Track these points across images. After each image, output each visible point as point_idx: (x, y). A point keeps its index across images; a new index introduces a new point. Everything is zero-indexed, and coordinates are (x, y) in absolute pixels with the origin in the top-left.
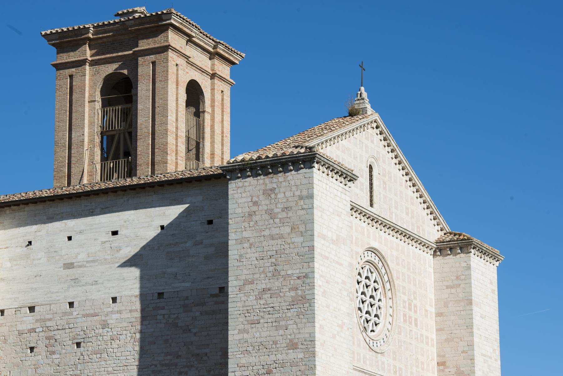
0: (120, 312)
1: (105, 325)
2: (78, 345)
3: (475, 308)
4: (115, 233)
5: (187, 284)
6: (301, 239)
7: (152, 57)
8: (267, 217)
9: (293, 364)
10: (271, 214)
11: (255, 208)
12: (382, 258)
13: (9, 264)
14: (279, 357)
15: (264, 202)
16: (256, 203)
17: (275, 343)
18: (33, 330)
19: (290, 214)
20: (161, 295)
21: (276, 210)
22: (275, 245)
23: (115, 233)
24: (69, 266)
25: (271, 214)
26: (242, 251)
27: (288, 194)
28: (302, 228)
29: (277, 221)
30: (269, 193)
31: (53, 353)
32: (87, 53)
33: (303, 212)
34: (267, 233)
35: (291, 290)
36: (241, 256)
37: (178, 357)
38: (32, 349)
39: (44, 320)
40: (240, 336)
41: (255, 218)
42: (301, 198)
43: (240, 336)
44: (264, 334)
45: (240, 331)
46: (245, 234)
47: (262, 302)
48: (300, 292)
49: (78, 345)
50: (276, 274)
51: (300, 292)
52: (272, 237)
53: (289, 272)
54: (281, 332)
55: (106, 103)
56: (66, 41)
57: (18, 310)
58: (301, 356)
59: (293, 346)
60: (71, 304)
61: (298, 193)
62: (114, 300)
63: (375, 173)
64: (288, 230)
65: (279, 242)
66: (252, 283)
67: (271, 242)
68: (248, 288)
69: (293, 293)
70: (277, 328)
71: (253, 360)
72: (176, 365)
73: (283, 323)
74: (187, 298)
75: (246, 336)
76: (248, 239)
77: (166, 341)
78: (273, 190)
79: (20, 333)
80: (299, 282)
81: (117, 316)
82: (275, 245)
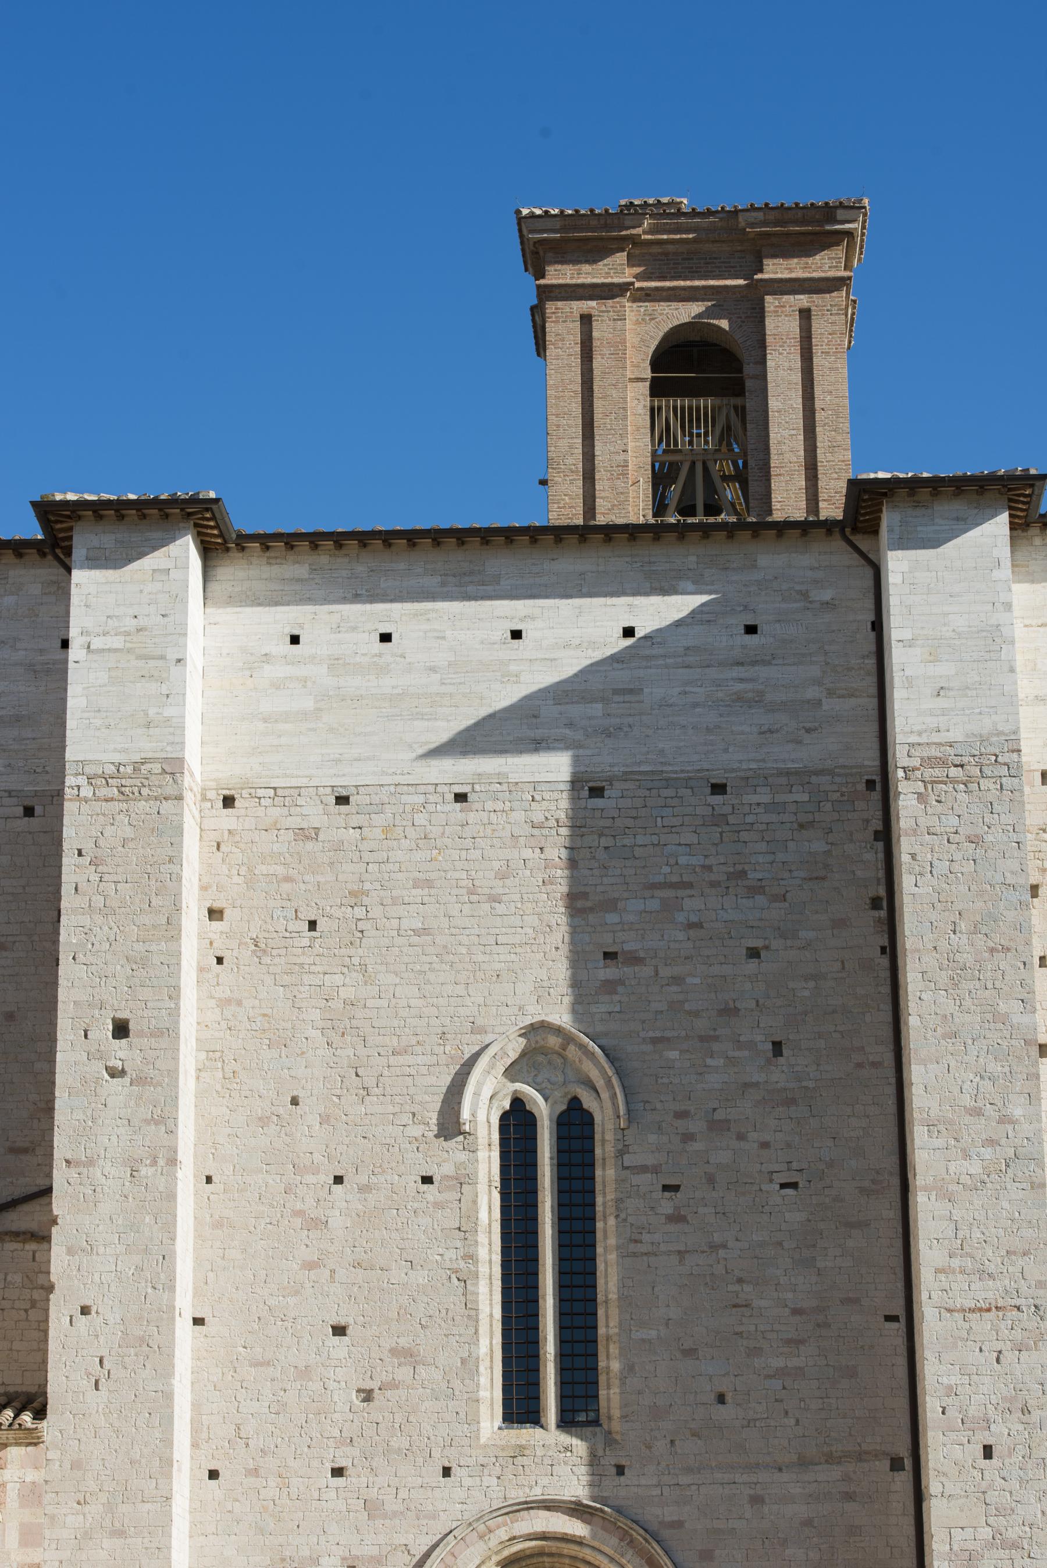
7: (803, 300)
32: (616, 269)
55: (657, 389)
56: (584, 236)
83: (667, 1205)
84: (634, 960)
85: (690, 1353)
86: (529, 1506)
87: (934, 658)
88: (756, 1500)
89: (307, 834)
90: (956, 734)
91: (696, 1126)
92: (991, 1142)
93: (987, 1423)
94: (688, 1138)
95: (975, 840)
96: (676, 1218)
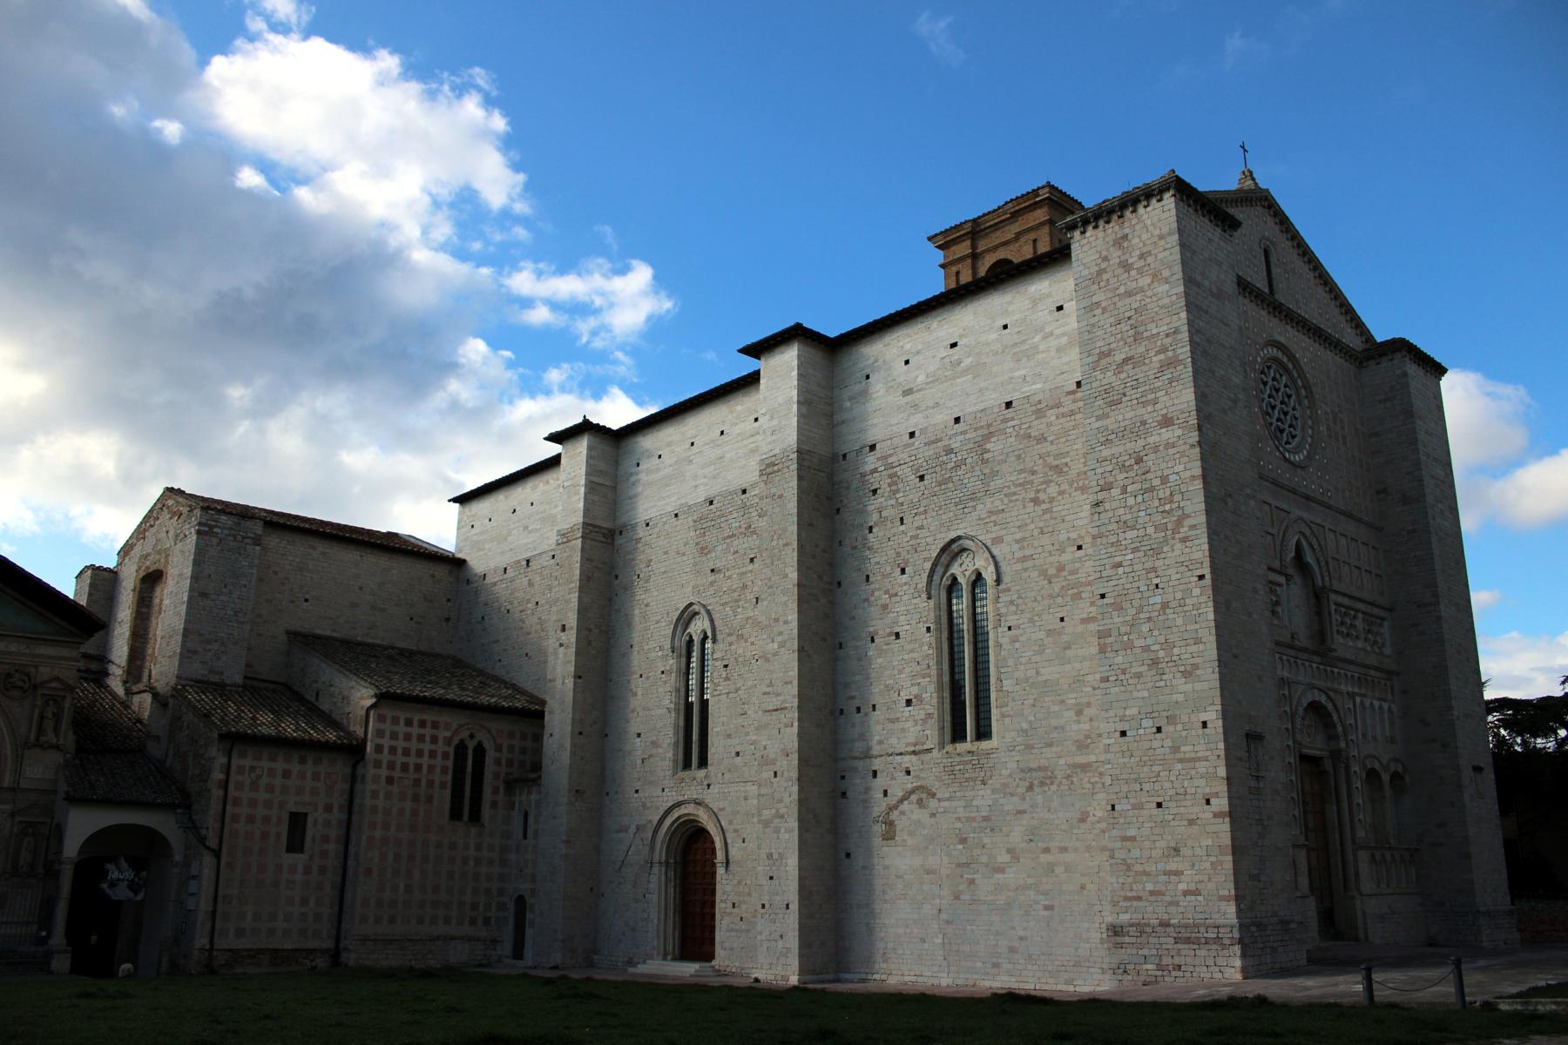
2: (922, 478)
3: (1419, 422)
4: (954, 345)
5: (1039, 386)
8: (1121, 270)
9: (1168, 445)
10: (1126, 267)
12: (1292, 358)
14: (1151, 440)
15: (1115, 255)
16: (1105, 259)
17: (1144, 423)
19: (1150, 260)
20: (1009, 405)
22: (1135, 302)
23: (954, 345)
25: (1126, 267)
26: (1092, 321)
27: (1144, 237)
29: (1133, 273)
31: (898, 491)
33: (1167, 253)
34: (1122, 290)
35: (1158, 353)
37: (1033, 473)
39: (886, 458)
40: (1099, 424)
41: (1105, 277)
42: (1161, 237)
43: (1099, 424)
44: (1128, 416)
45: (1099, 418)
46: (1095, 299)
47: (1123, 376)
48: (1170, 354)
50: (1137, 338)
51: (1170, 354)
52: (1129, 294)
54: (1150, 409)
58: (1179, 432)
59: (1167, 422)
61: (1157, 232)
63: (1273, 259)
65: (1139, 297)
66: (1109, 355)
67: (1128, 301)
68: (1103, 362)
69: (1162, 357)
71: (1116, 450)
72: (1032, 482)
77: (1019, 457)
78: (1125, 237)
80: (1169, 340)
81: (961, 438)
82: (1135, 302)
85: (729, 736)
86: (678, 805)
87: (772, 418)
90: (777, 451)
92: (781, 633)
93: (774, 762)
95: (781, 496)
96: (727, 679)
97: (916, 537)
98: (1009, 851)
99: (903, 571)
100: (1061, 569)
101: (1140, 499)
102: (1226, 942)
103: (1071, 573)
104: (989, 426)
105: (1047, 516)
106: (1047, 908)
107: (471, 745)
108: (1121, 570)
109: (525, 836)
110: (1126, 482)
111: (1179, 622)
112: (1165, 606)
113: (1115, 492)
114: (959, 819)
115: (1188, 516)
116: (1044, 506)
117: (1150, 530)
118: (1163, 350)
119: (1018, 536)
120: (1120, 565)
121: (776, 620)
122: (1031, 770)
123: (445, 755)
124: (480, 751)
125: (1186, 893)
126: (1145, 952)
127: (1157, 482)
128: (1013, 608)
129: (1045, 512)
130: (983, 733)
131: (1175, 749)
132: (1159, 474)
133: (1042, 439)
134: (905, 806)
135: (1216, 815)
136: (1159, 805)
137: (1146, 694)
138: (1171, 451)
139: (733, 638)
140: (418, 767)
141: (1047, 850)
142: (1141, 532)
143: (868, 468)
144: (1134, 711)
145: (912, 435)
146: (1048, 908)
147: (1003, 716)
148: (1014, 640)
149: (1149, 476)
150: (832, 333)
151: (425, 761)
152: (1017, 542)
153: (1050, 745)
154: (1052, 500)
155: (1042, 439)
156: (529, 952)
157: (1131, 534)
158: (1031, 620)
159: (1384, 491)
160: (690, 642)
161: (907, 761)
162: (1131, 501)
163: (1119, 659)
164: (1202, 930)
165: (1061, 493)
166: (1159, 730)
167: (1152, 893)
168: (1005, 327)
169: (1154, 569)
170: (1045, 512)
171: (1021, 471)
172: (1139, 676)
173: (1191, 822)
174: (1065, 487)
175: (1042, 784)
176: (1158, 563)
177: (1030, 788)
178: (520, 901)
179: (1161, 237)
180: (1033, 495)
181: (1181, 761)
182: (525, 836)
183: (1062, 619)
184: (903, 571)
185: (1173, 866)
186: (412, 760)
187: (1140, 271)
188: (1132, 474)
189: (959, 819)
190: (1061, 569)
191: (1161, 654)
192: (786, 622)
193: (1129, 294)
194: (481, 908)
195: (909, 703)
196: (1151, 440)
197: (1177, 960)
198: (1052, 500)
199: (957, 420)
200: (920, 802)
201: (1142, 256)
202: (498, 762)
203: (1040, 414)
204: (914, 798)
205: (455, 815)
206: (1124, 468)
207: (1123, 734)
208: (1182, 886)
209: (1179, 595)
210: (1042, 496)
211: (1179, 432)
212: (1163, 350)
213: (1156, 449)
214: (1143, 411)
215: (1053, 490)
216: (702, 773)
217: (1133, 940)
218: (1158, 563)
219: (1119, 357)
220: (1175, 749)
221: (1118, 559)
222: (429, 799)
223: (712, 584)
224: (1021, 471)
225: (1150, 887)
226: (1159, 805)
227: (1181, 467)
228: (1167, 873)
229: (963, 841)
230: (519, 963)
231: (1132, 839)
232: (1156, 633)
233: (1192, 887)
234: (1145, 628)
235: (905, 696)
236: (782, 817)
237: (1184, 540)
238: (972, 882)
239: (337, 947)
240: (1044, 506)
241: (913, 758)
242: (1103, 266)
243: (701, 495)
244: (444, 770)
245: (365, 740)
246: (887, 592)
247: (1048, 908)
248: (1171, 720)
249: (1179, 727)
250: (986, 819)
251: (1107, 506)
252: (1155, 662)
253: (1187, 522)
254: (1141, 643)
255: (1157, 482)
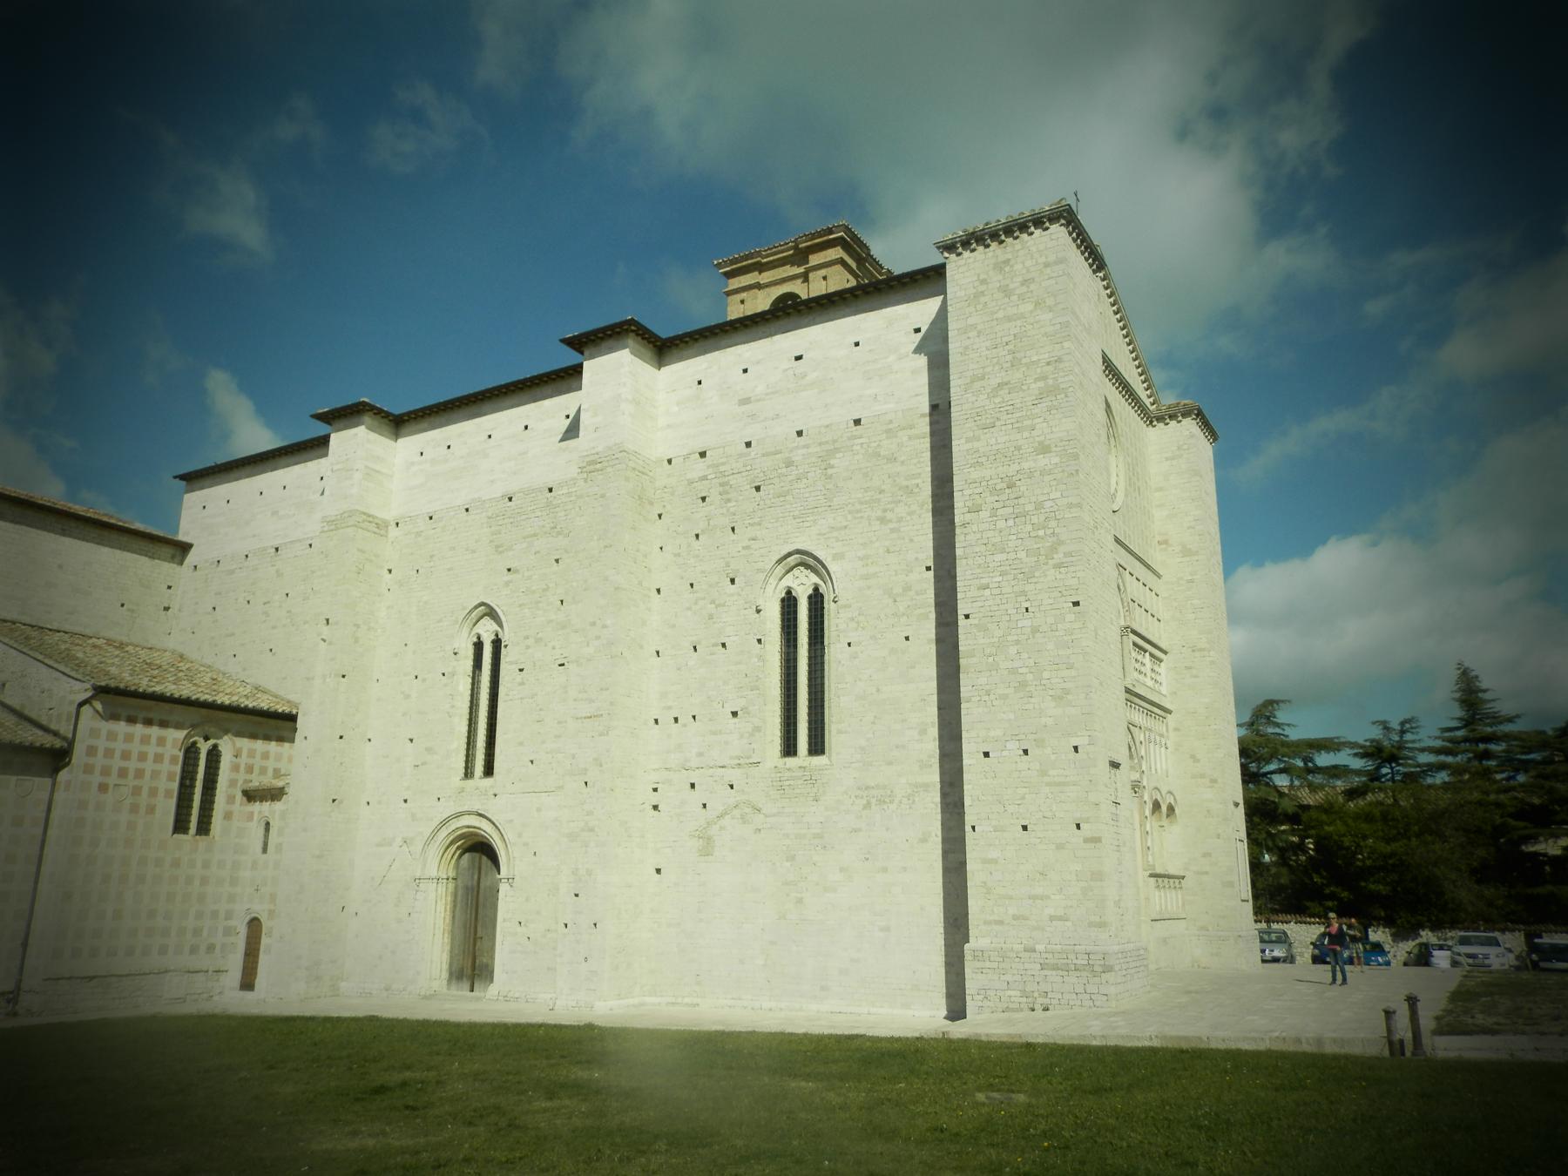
0: (807, 446)
1: (789, 463)
2: (758, 489)
4: (798, 358)
6: (1051, 315)
7: (823, 272)
10: (1006, 291)
11: (983, 288)
13: (676, 409)
14: (1026, 465)
16: (983, 282)
17: (1018, 448)
18: (704, 478)
19: (1032, 287)
20: (857, 422)
21: (1012, 286)
23: (798, 358)
24: (745, 401)
27: (1028, 263)
28: (1050, 302)
29: (1014, 298)
30: (1000, 267)
31: (729, 500)
34: (1000, 314)
35: (1036, 380)
36: (966, 348)
38: (704, 499)
39: (718, 466)
40: (969, 446)
41: (983, 299)
42: (1047, 265)
43: (969, 446)
45: (968, 440)
46: (971, 321)
47: (997, 400)
48: (1050, 382)
49: (758, 489)
51: (1050, 382)
52: (1009, 319)
53: (1035, 358)
54: (1026, 434)
57: (686, 457)
58: (1057, 460)
59: (1044, 449)
60: (748, 444)
61: (1043, 260)
62: (800, 433)
64: (1030, 307)
65: (1019, 323)
66: (983, 378)
68: (977, 385)
69: (1041, 384)
70: (1020, 430)
72: (879, 500)
73: (1028, 422)
74: (891, 422)
75: (976, 444)
76: (974, 326)
77: (866, 475)
78: (1007, 262)
79: (691, 482)
80: (1050, 368)
81: (804, 451)
83: (519, 677)
84: (517, 571)
85: (521, 744)
86: (461, 814)
88: (539, 810)
89: (419, 534)
90: (600, 449)
91: (531, 641)
92: (598, 638)
94: (528, 647)
95: (603, 496)
96: (522, 684)
97: (747, 548)
98: (841, 870)
99: (733, 581)
100: (907, 588)
101: (1011, 523)
102: (1097, 968)
103: (917, 594)
104: (835, 441)
105: (894, 535)
106: (882, 929)
107: (204, 747)
108: (987, 592)
109: (265, 850)
110: (996, 505)
111: (1050, 646)
112: (1035, 630)
113: (984, 514)
114: (787, 836)
115: (1061, 543)
116: (891, 526)
117: (1022, 555)
118: (1044, 378)
119: (860, 554)
120: (986, 587)
121: (594, 624)
122: (867, 788)
123: (173, 760)
124: (214, 756)
125: (1052, 918)
126: (1008, 977)
127: (1030, 507)
128: (853, 625)
129: (893, 530)
130: (817, 747)
131: (1043, 773)
132: (1033, 499)
133: (892, 459)
134: (727, 821)
135: (1086, 841)
136: (1025, 828)
137: (1012, 716)
138: (1047, 478)
139: (531, 641)
140: (139, 774)
141: (885, 870)
142: (1012, 556)
143: (695, 475)
144: (999, 733)
145: (748, 444)
146: (887, 929)
147: (840, 732)
148: (854, 657)
149: (1021, 501)
150: (664, 335)
151: (149, 766)
152: (860, 559)
153: (890, 763)
154: (900, 520)
155: (892, 459)
156: (261, 981)
157: (998, 557)
158: (873, 637)
159: (1166, 542)
160: (479, 646)
161: (734, 775)
162: (1001, 524)
163: (983, 680)
164: (1072, 956)
165: (911, 514)
166: (1026, 752)
167: (1015, 917)
168: (857, 344)
169: (1024, 593)
170: (893, 530)
171: (866, 490)
172: (1004, 697)
173: (1060, 847)
174: (914, 507)
175: (881, 802)
176: (1028, 587)
177: (868, 805)
178: (254, 925)
179: (1047, 265)
180: (879, 513)
181: (1048, 784)
182: (265, 850)
183: (907, 638)
184: (733, 581)
185: (1039, 891)
186: (132, 765)
187: (1021, 297)
188: (1004, 497)
189: (787, 836)
190: (907, 588)
191: (1030, 677)
192: (605, 626)
193: (1009, 319)
194: (205, 933)
195: (735, 714)
196: (1026, 465)
197: (1043, 987)
198: (900, 520)
199: (800, 433)
200: (744, 819)
201: (1025, 282)
202: (236, 768)
203: (889, 433)
204: (737, 812)
205: (180, 826)
206: (994, 491)
207: (986, 755)
208: (1051, 911)
209: (1050, 620)
210: (889, 515)
211: (1057, 460)
212: (1044, 378)
213: (1031, 475)
214: (1018, 436)
215: (901, 510)
216: (488, 781)
217: (995, 965)
218: (1028, 587)
219: (995, 382)
220: (1043, 773)
221: (984, 581)
222: (151, 810)
223: (507, 584)
224: (866, 490)
225: (1011, 911)
226: (1025, 828)
227: (1058, 495)
228: (1033, 897)
229: (792, 858)
230: (248, 995)
231: (995, 861)
232: (1025, 656)
233: (1060, 912)
234: (1013, 650)
235: (729, 709)
236: (592, 830)
237: (1058, 566)
238: (800, 901)
239: (18, 987)
240: (891, 526)
241: (738, 771)
242: (983, 288)
243: (499, 490)
244: (170, 777)
245: (71, 743)
246: (713, 602)
247: (887, 929)
248: (1040, 743)
249: (1048, 751)
250: (817, 836)
251: (975, 528)
252: (1023, 685)
253: (1062, 549)
254: (1009, 664)
255: (1030, 507)
